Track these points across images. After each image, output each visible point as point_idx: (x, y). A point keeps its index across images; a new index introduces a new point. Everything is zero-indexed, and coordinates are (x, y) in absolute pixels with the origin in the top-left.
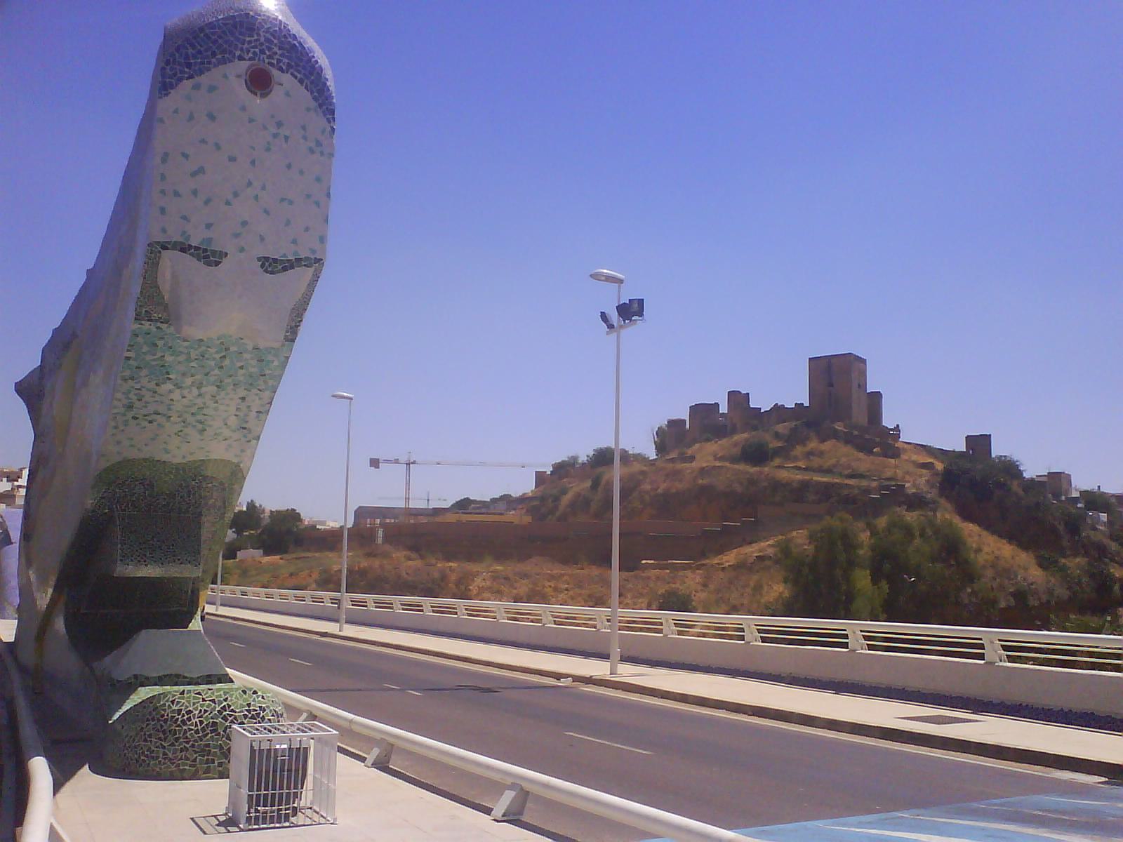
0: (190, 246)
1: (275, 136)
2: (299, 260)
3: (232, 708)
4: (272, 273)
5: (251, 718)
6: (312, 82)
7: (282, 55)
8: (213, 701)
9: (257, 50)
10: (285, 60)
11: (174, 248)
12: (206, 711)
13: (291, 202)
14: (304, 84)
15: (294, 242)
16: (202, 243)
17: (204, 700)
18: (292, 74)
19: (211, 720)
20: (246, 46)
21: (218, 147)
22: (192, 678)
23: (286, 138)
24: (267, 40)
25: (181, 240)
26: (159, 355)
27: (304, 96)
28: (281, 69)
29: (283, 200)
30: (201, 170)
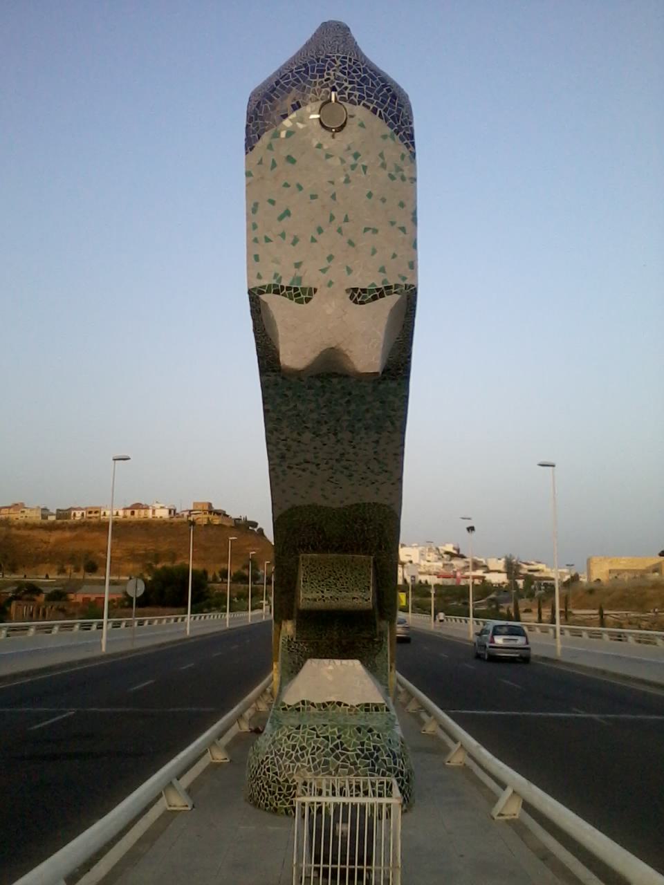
0: (282, 287)
1: (353, 167)
2: (388, 288)
3: (345, 746)
4: (362, 303)
5: (364, 758)
6: (385, 110)
7: (353, 89)
8: (326, 738)
10: (357, 93)
11: (269, 291)
12: (318, 748)
13: (375, 231)
14: (378, 113)
15: (382, 270)
16: (291, 284)
17: (318, 737)
18: (364, 105)
19: (323, 759)
20: (318, 87)
21: (300, 187)
22: (352, 706)
23: (365, 168)
25: (274, 282)
26: (292, 405)
27: (379, 126)
28: (352, 102)
29: (366, 230)
30: (287, 213)
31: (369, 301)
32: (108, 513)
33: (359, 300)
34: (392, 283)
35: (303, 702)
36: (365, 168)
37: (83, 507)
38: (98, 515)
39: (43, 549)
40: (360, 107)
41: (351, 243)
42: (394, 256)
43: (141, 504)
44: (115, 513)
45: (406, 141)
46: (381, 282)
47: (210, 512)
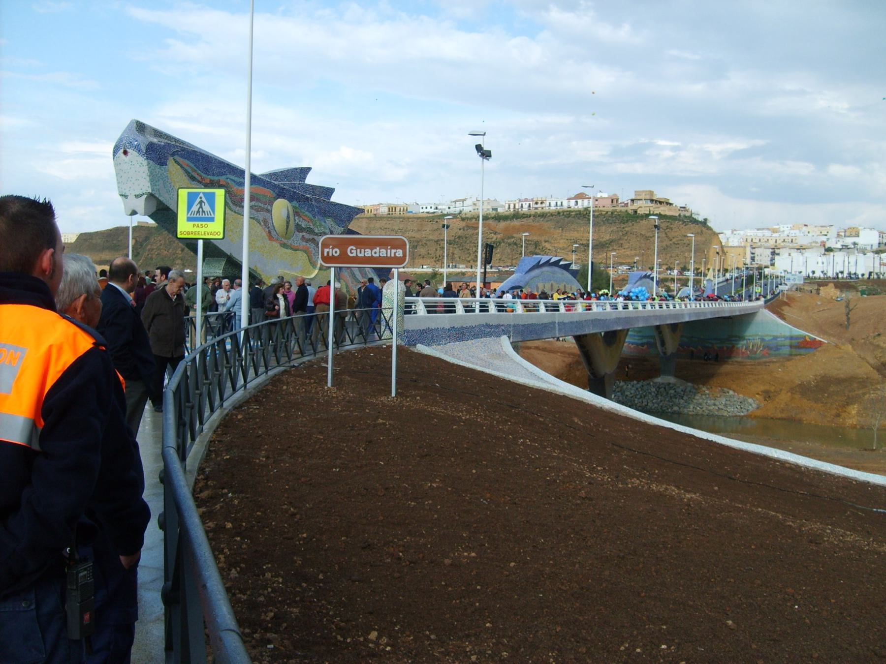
32: (553, 204)
37: (529, 198)
39: (493, 240)
43: (584, 194)
44: (559, 204)
47: (652, 201)
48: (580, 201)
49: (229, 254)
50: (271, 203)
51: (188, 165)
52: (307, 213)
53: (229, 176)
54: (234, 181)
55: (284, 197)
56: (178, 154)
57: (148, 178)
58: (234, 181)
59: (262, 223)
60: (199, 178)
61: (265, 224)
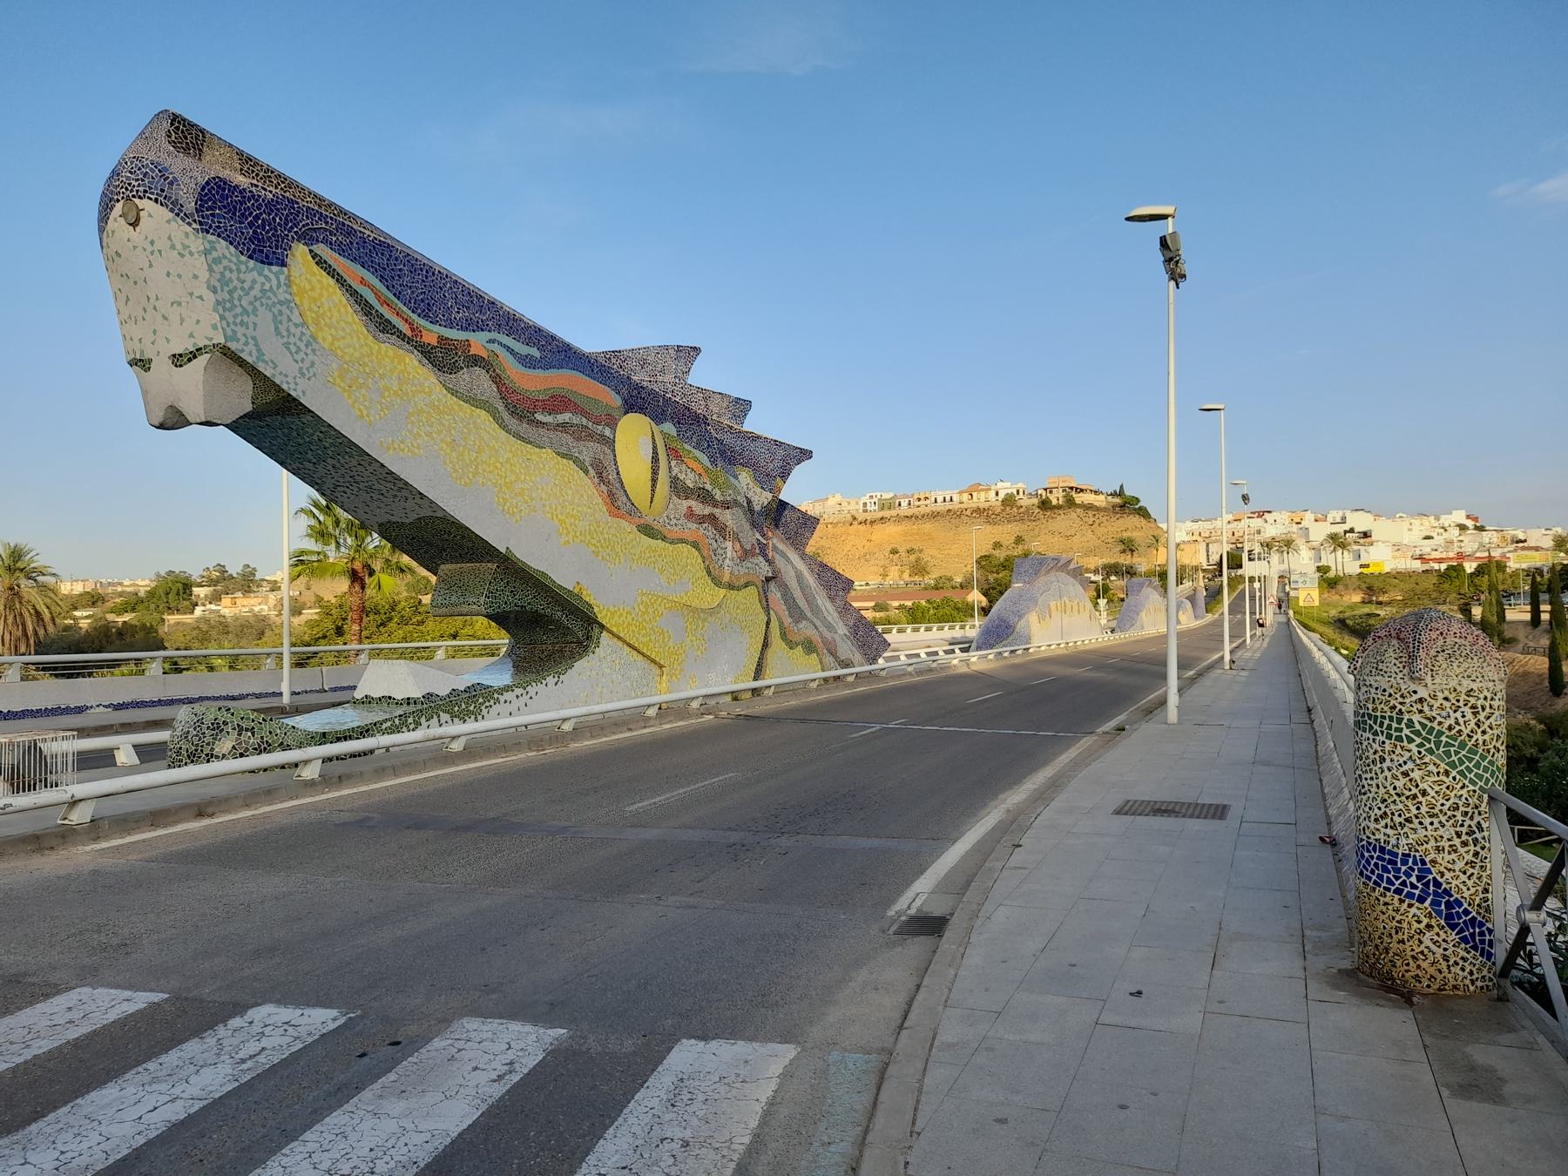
1: (152, 253)
4: (181, 366)
9: (123, 190)
15: (191, 335)
18: (149, 198)
24: (128, 178)
28: (140, 197)
29: (172, 304)
31: (185, 364)
33: (178, 364)
34: (201, 345)
35: (366, 696)
36: (160, 251)
38: (928, 502)
40: (146, 200)
41: (165, 318)
42: (198, 322)
44: (948, 499)
45: (188, 220)
46: (192, 344)
48: (975, 494)
49: (504, 551)
50: (612, 423)
51: (363, 282)
52: (697, 453)
53: (494, 335)
54: (511, 351)
55: (641, 410)
56: (325, 241)
57: (210, 298)
58: (511, 351)
59: (592, 472)
60: (405, 328)
61: (600, 475)
